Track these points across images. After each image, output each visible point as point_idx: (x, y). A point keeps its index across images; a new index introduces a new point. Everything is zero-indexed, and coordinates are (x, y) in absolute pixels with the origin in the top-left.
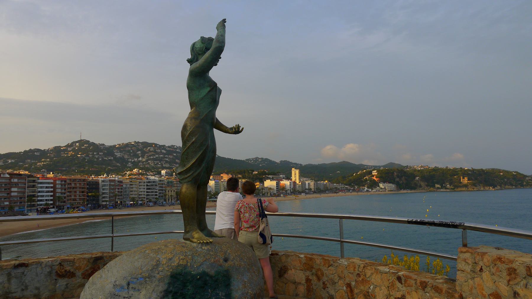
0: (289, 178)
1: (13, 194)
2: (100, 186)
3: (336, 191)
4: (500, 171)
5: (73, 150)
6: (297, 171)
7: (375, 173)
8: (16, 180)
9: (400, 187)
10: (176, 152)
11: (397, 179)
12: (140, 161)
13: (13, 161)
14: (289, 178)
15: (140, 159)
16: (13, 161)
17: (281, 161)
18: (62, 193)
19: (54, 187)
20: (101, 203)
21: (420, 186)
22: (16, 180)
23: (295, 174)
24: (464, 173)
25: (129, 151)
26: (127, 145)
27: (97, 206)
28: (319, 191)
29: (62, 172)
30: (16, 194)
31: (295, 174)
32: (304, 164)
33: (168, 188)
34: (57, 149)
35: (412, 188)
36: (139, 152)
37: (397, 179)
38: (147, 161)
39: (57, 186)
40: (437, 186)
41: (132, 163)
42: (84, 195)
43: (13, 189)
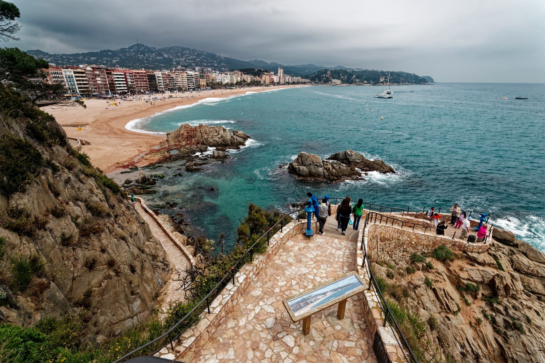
0: (276, 74)
1: (98, 82)
2: (156, 77)
3: (305, 83)
4: (404, 73)
5: (134, 51)
6: (282, 70)
7: (329, 72)
8: (98, 72)
9: (343, 82)
10: (204, 55)
11: (342, 77)
12: (180, 61)
13: (94, 58)
14: (276, 74)
15: (181, 59)
16: (94, 58)
17: (271, 63)
18: (132, 82)
19: (125, 78)
20: (158, 89)
21: (355, 82)
22: (98, 72)
23: (281, 71)
24: (383, 74)
25: (172, 53)
26: (170, 49)
27: (157, 91)
28: (294, 83)
29: (129, 67)
30: (100, 82)
31: (281, 71)
32: (285, 65)
33: (201, 80)
34: (123, 50)
35: (350, 83)
36: (179, 54)
37: (342, 77)
38: (185, 60)
39: (127, 77)
40: (365, 82)
41: (176, 62)
42: (146, 84)
43: (98, 79)
